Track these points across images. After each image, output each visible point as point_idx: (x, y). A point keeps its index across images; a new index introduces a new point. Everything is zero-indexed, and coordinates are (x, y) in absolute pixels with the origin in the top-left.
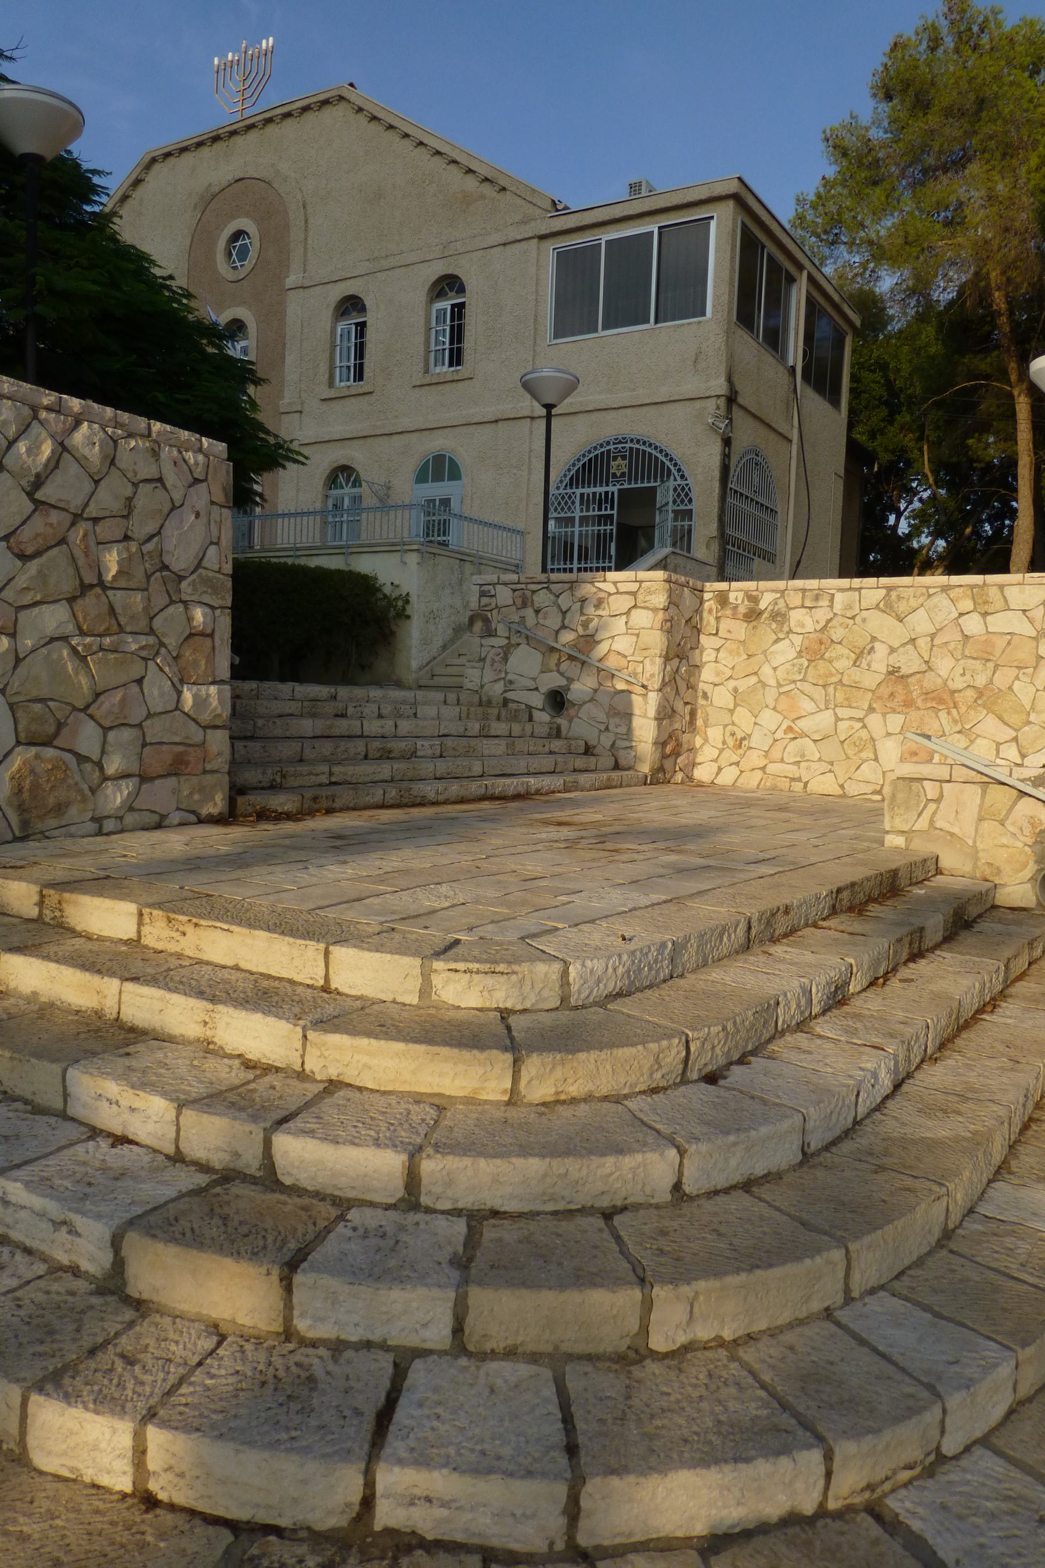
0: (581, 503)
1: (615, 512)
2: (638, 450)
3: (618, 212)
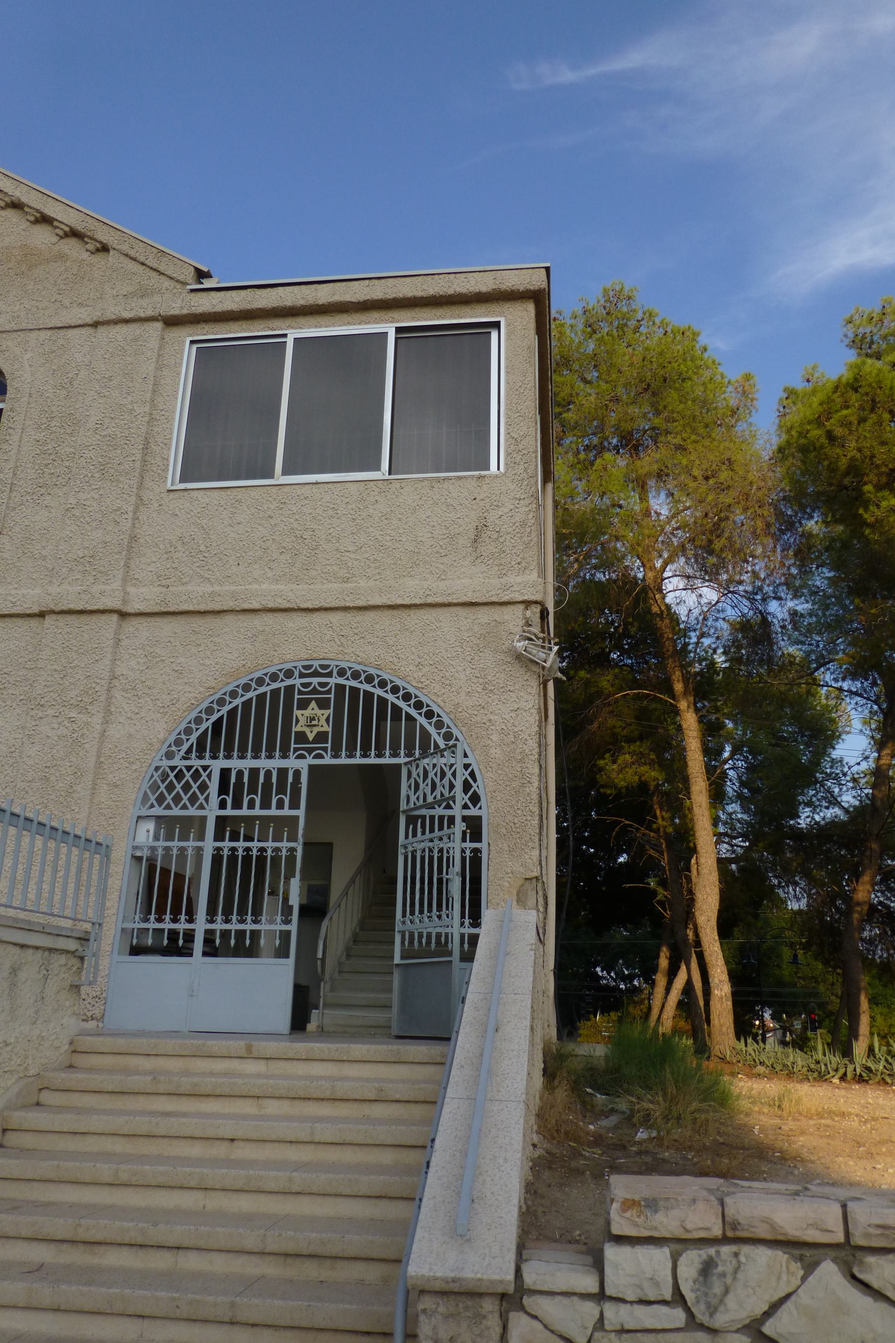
0: (223, 788)
1: (301, 813)
2: (354, 691)
3: (323, 295)
